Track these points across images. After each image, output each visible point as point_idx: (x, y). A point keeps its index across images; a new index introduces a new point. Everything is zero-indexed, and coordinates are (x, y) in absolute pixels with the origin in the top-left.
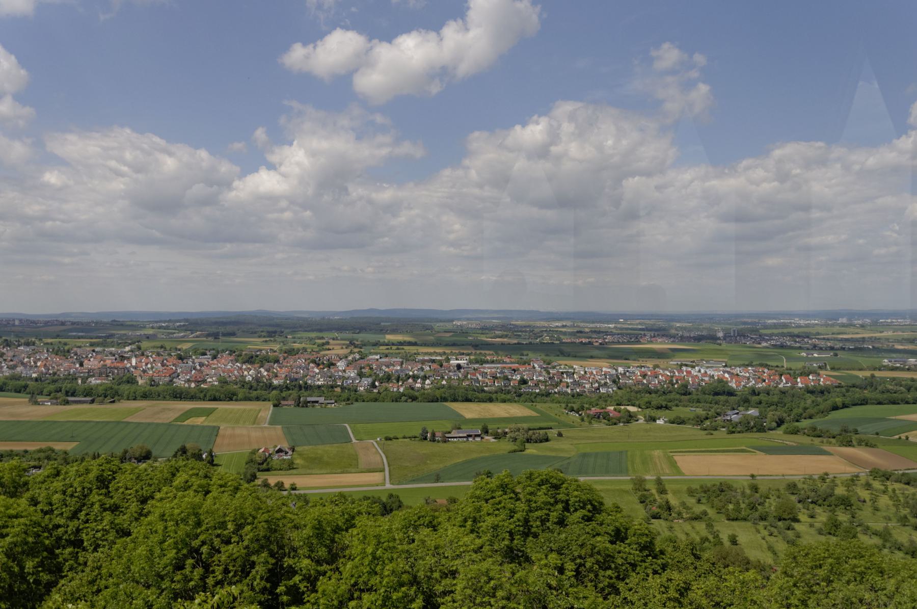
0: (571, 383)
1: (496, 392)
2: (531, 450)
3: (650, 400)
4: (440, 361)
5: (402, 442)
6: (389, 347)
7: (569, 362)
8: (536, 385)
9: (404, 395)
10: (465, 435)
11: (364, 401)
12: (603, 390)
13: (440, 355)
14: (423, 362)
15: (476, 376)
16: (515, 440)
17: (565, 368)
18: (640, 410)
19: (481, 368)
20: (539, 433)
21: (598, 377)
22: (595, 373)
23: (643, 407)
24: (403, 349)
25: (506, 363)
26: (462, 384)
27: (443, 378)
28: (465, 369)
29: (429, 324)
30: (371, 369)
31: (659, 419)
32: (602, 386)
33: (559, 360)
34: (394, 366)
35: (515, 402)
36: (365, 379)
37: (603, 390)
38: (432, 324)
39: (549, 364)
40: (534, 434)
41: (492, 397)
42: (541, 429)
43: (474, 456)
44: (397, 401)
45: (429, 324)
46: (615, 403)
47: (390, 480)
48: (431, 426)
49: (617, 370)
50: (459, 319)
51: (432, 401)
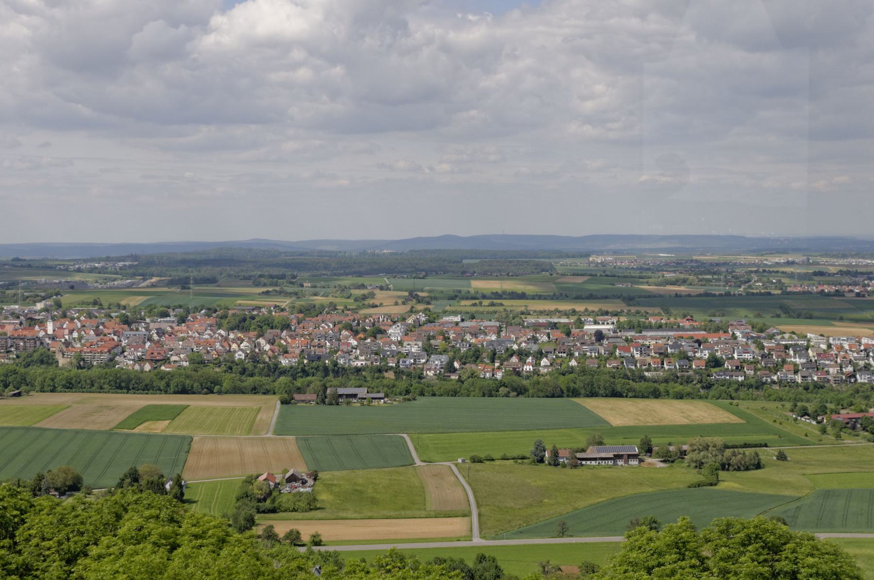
0: (803, 364)
1: (666, 381)
2: (729, 482)
4: (565, 325)
5: (500, 465)
6: (477, 301)
7: (800, 328)
8: (737, 367)
9: (504, 385)
10: (611, 455)
11: (434, 395)
12: (861, 379)
13: (566, 314)
14: (536, 327)
16: (700, 465)
17: (791, 338)
19: (639, 338)
20: (744, 453)
21: (852, 356)
22: (846, 347)
24: (501, 305)
25: (683, 329)
26: (605, 366)
27: (571, 355)
28: (611, 340)
29: (547, 260)
30: (447, 339)
32: (860, 370)
33: (780, 324)
34: (486, 334)
35: (701, 398)
37: (861, 379)
38: (552, 261)
39: (761, 331)
40: (734, 454)
41: (658, 390)
42: (746, 446)
43: (628, 491)
44: (491, 395)
45: (547, 260)
47: (481, 530)
48: (551, 439)
50: (599, 253)
51: (553, 396)
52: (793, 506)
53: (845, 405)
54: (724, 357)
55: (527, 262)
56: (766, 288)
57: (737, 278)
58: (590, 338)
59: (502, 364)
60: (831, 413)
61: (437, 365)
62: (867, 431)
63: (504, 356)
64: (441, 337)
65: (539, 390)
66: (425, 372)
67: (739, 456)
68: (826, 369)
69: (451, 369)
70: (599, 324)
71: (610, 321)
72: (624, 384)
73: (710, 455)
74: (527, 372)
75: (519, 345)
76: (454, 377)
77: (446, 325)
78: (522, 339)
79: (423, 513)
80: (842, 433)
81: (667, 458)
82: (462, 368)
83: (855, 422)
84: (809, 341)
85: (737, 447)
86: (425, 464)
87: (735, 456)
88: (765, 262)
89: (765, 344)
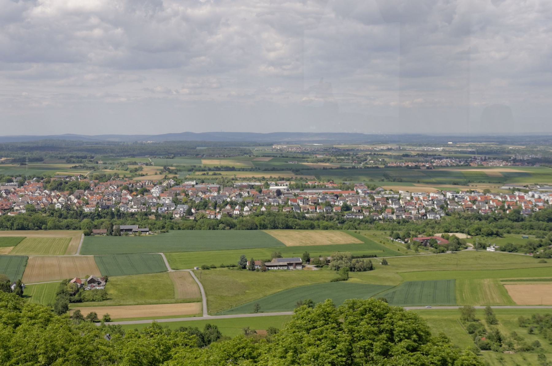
0: (397, 209)
1: (318, 219)
2: (355, 278)
3: (480, 226)
4: (258, 186)
5: (220, 271)
6: (205, 172)
7: (395, 188)
8: (359, 211)
9: (222, 223)
10: (286, 263)
11: (179, 229)
12: (430, 217)
13: (259, 180)
14: (241, 188)
15: (296, 201)
16: (338, 268)
17: (390, 194)
18: (469, 237)
19: (302, 194)
20: (363, 261)
21: (425, 203)
22: (421, 198)
23: (473, 234)
24: (220, 174)
26: (282, 211)
27: (262, 204)
28: (286, 195)
29: (248, 148)
30: (187, 195)
31: (489, 246)
32: (429, 212)
33: (384, 185)
34: (211, 192)
35: (338, 229)
36: (181, 206)
38: (251, 148)
39: (373, 189)
40: (357, 262)
41: (313, 225)
42: (364, 257)
44: (214, 229)
45: (248, 148)
46: (443, 230)
47: (208, 310)
48: (250, 255)
49: (445, 196)
51: (251, 229)
52: (392, 291)
53: (421, 232)
54: (352, 205)
55: (235, 148)
56: (376, 164)
57: (359, 158)
58: (273, 194)
59: (220, 210)
60: (413, 237)
61: (181, 211)
62: (433, 247)
63: (222, 205)
64: (184, 194)
65: (243, 225)
66: (174, 215)
67: (360, 263)
68: (410, 211)
69: (190, 213)
70: (278, 185)
71: (285, 184)
72: (293, 221)
73: (343, 262)
74: (236, 214)
75: (231, 198)
76: (192, 218)
77: (187, 187)
78: (233, 195)
79: (173, 300)
80: (419, 248)
81: (318, 265)
82: (197, 213)
83: (426, 242)
84: (400, 195)
85: (359, 257)
86: (174, 271)
87: (358, 263)
88: (375, 149)
89: (375, 197)
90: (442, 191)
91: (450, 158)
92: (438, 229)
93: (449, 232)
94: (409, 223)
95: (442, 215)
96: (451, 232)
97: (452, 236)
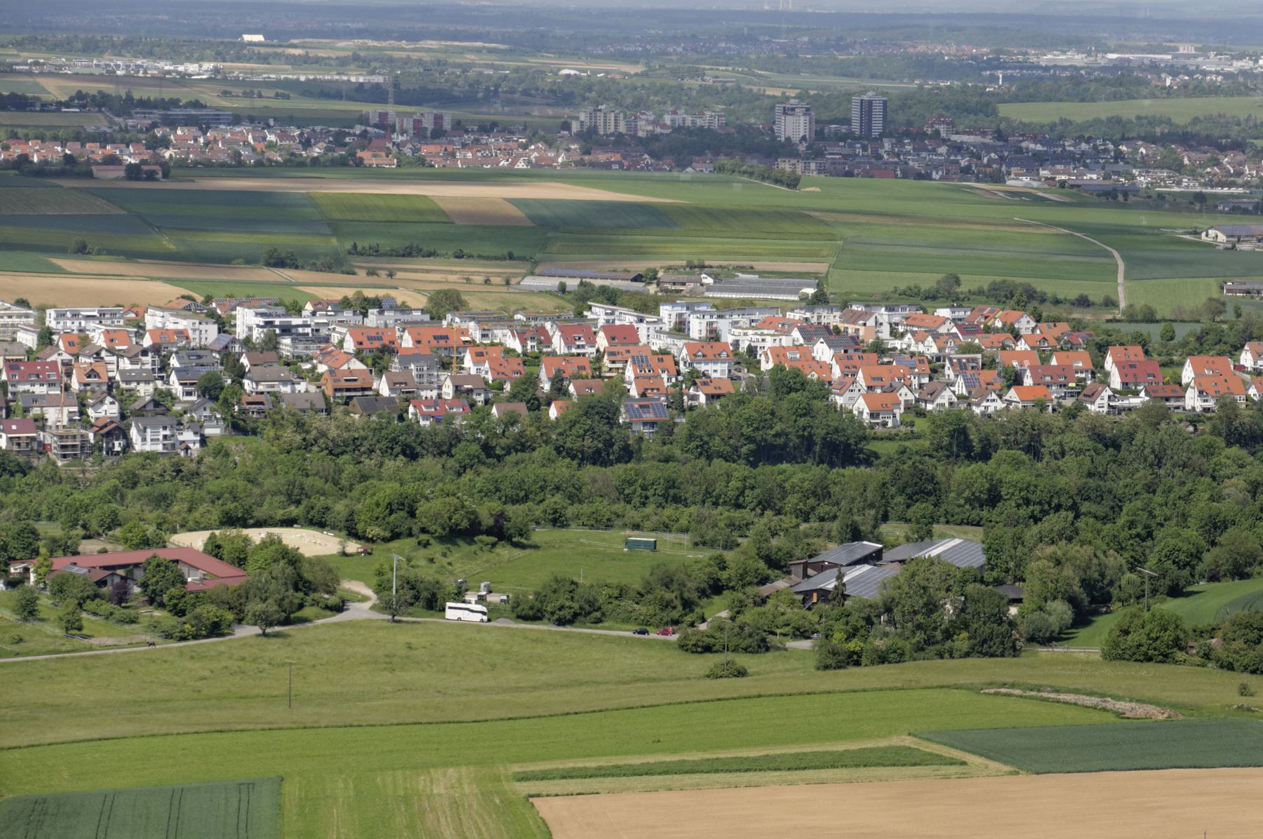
3: (410, 488)
12: (145, 440)
18: (353, 547)
21: (117, 367)
22: (99, 340)
23: (373, 531)
31: (459, 595)
32: (140, 413)
37: (145, 440)
46: (215, 516)
49: (224, 326)
53: (94, 526)
60: (52, 552)
62: (162, 605)
68: (36, 411)
80: (84, 615)
83: (123, 578)
90: (208, 300)
91: (252, 120)
92: (190, 510)
93: (246, 526)
94: (31, 477)
95: (212, 431)
96: (259, 524)
97: (264, 545)
